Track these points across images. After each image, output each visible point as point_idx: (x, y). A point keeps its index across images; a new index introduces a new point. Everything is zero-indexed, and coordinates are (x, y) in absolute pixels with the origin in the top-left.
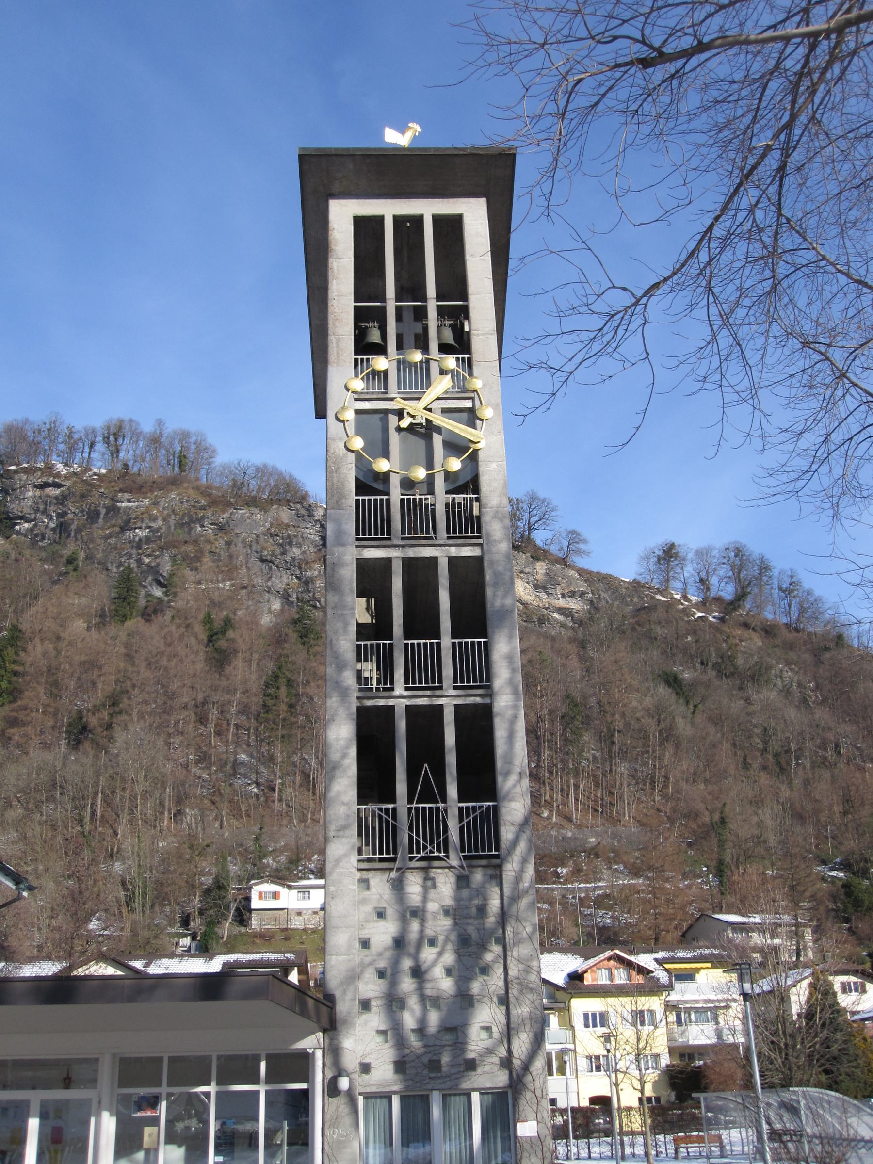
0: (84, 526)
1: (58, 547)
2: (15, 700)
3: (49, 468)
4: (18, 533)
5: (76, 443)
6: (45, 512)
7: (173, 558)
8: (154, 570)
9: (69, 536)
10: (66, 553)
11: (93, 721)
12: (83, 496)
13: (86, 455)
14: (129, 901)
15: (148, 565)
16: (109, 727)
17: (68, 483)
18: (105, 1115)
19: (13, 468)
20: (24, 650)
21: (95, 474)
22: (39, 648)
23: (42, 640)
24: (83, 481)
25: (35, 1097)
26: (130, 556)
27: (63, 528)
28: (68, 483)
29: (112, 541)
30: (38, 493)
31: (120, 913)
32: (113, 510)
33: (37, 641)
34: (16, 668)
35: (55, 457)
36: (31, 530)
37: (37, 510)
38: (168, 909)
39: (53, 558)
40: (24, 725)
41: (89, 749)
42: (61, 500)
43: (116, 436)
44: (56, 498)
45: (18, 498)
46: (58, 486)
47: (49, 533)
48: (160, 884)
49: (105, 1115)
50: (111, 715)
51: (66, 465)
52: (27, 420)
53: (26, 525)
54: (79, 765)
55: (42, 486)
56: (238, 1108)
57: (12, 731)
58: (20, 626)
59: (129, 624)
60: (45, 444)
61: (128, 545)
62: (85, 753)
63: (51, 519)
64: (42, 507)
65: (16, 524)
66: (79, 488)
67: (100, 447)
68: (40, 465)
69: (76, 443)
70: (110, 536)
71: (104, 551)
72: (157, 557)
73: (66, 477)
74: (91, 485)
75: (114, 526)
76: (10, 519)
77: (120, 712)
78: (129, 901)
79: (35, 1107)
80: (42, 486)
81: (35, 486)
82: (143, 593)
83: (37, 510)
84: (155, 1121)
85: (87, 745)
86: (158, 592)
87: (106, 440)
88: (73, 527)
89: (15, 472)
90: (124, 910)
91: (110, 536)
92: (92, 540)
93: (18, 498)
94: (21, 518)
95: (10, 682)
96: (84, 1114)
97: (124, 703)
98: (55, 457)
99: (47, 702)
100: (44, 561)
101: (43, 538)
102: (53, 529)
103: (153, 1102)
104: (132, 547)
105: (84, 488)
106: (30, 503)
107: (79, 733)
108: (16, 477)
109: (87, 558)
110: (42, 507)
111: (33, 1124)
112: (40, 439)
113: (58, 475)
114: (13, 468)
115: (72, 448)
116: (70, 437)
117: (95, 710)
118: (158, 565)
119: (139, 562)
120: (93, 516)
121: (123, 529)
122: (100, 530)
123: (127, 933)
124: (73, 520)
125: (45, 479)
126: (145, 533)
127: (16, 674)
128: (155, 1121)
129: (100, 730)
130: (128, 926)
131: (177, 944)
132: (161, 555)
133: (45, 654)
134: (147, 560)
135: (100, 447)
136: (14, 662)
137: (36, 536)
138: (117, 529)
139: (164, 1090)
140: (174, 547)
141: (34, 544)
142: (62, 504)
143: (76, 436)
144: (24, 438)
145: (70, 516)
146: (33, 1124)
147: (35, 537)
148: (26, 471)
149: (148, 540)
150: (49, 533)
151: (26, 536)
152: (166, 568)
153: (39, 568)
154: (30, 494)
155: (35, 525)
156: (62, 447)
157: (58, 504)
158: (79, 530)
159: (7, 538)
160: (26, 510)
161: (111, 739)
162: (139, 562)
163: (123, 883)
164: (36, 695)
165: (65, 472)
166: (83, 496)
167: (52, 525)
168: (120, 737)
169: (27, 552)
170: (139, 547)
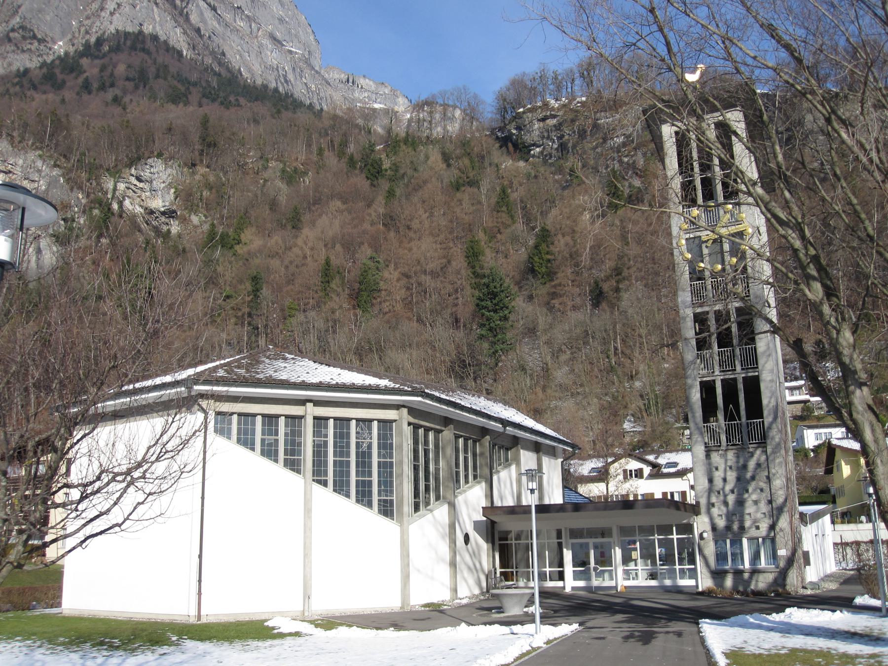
0: (577, 142)
1: (562, 162)
2: (552, 280)
3: (546, 105)
4: (534, 156)
5: (560, 82)
6: (548, 138)
7: (644, 155)
8: (633, 166)
9: (568, 152)
10: (569, 164)
11: (606, 287)
12: (573, 121)
13: (569, 90)
14: (647, 408)
15: (627, 163)
16: (617, 290)
17: (560, 113)
18: (617, 548)
19: (521, 110)
20: (553, 244)
21: (578, 102)
22: (562, 242)
23: (564, 236)
24: (571, 109)
25: (591, 541)
26: (614, 160)
27: (563, 147)
28: (560, 113)
29: (599, 150)
30: (541, 124)
31: (643, 417)
32: (596, 126)
33: (560, 236)
34: (549, 257)
35: (548, 96)
36: (542, 152)
37: (543, 137)
38: (674, 411)
39: (560, 170)
40: (561, 296)
41: (606, 308)
42: (558, 127)
43: (588, 71)
44: (555, 126)
45: (529, 131)
46: (554, 117)
47: (554, 152)
48: (666, 397)
49: (617, 548)
50: (618, 282)
51: (557, 100)
52: (524, 73)
53: (538, 150)
54: (602, 319)
55: (543, 120)
56: (667, 544)
57: (553, 301)
58: (547, 228)
59: (620, 212)
60: (540, 88)
61: (611, 151)
62: (604, 311)
63: (554, 142)
64: (546, 134)
65: (531, 150)
66: (570, 116)
67: (578, 82)
68: (539, 104)
69: (560, 82)
70: (596, 147)
71: (594, 159)
72: (632, 156)
73: (559, 109)
74: (577, 111)
75: (597, 139)
76: (525, 147)
77: (624, 279)
78: (647, 408)
79: (591, 546)
80: (543, 120)
81: (539, 120)
82: (627, 184)
83: (543, 137)
84: (635, 549)
85: (604, 305)
86: (637, 183)
87: (582, 75)
88: (570, 145)
89: (524, 112)
90: (645, 414)
91: (596, 147)
92: (585, 152)
93: (529, 131)
94: (534, 145)
95: (547, 267)
96: (610, 547)
97: (625, 273)
98: (548, 96)
99: (573, 278)
100: (554, 173)
101: (551, 157)
102: (557, 149)
103: (634, 542)
104: (613, 152)
105: (573, 115)
106: (537, 133)
107: (598, 297)
108: (525, 116)
109: (584, 166)
110: (546, 134)
111: (592, 553)
112: (535, 85)
113: (553, 109)
114: (521, 110)
115: (559, 88)
116: (556, 78)
117: (607, 278)
118: (634, 162)
119: (620, 162)
120: (582, 134)
121: (605, 140)
122: (589, 144)
123: (649, 429)
124: (569, 140)
125: (544, 114)
126: (622, 139)
127: (549, 261)
128: (635, 549)
129: (611, 293)
130: (649, 424)
131: (683, 434)
132: (635, 155)
133: (567, 244)
134: (626, 160)
135: (578, 82)
136: (548, 253)
137: (546, 156)
138: (601, 141)
139: (637, 538)
140: (644, 145)
141: (545, 162)
142: (559, 129)
143: (560, 78)
144: (525, 87)
145: (567, 137)
146: (592, 553)
147: (545, 157)
148: (530, 110)
149: (624, 144)
150: (554, 152)
151: (539, 157)
152: (641, 162)
153: (551, 180)
154: (536, 126)
155: (544, 149)
156: (551, 87)
157: (557, 130)
158: (574, 147)
159: (527, 161)
160: (536, 139)
161: (619, 299)
162: (620, 162)
163: (641, 396)
164: (565, 274)
165: (557, 105)
166: (573, 121)
167: (555, 146)
168: (625, 296)
169: (542, 169)
170: (619, 151)
